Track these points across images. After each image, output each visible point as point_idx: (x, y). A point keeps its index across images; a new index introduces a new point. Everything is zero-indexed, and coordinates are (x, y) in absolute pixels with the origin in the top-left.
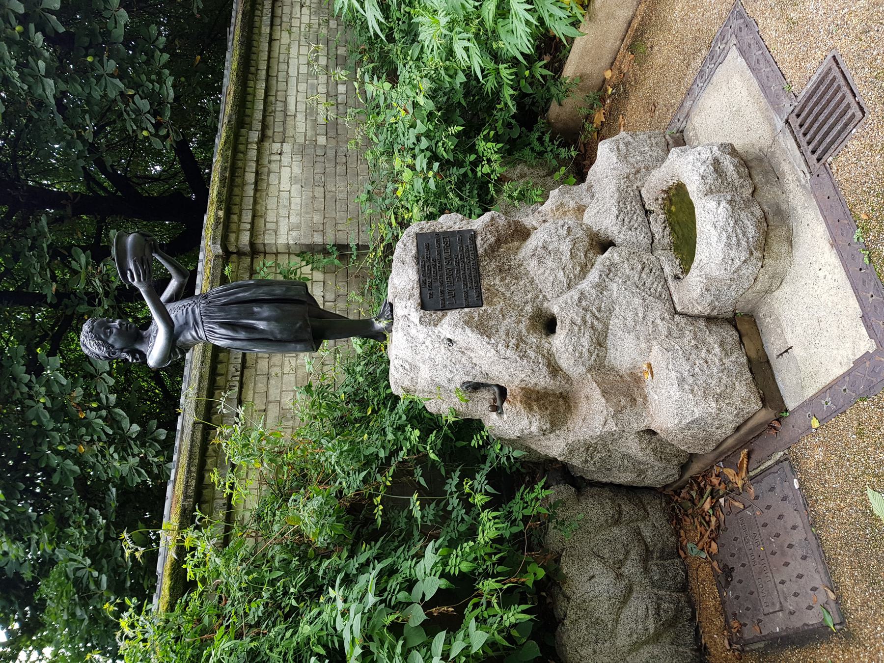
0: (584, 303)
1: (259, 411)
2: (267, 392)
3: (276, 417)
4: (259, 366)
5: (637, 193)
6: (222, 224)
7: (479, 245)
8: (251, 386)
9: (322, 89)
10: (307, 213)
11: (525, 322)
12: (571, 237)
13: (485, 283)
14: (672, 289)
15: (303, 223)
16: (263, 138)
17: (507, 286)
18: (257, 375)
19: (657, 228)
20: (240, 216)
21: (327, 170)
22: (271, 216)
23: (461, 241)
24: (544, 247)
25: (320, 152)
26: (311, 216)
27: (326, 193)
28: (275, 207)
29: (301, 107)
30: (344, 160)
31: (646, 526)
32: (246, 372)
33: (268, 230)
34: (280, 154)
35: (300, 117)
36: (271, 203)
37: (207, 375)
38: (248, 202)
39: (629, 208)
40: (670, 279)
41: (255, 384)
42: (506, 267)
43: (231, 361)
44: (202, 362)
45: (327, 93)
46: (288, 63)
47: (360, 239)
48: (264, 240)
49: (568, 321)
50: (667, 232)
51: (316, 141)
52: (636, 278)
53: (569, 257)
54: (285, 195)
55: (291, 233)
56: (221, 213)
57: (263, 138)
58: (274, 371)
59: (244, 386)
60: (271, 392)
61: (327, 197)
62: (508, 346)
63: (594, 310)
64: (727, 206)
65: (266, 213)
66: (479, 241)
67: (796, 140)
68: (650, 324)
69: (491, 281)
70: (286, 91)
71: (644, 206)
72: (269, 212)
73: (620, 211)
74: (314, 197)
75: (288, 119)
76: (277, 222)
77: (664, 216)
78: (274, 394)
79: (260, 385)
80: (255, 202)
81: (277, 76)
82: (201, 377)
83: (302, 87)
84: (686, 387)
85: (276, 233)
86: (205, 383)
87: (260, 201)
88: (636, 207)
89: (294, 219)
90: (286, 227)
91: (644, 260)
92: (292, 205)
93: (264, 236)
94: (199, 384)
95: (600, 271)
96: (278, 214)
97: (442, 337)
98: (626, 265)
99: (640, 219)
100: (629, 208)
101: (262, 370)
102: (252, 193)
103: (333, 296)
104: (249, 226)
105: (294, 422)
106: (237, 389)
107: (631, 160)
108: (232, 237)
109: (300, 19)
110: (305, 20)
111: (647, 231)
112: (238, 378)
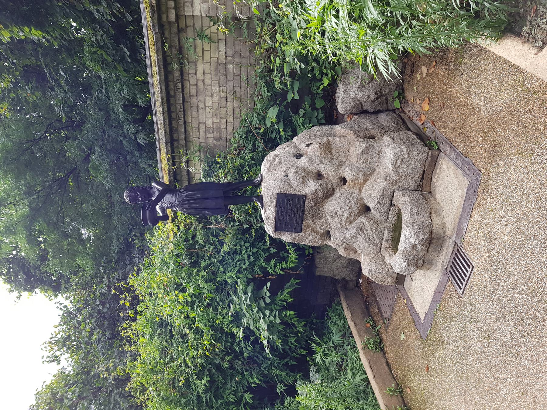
2: (198, 117)
3: (204, 131)
4: (192, 101)
5: (392, 194)
6: (156, 12)
7: (306, 206)
8: (189, 113)
11: (318, 237)
12: (350, 210)
13: (304, 223)
14: (383, 243)
17: (315, 223)
18: (191, 107)
19: (391, 215)
23: (299, 201)
24: (336, 213)
32: (185, 103)
37: (167, 117)
39: (384, 201)
40: (384, 239)
41: (191, 112)
42: (316, 214)
43: (177, 102)
44: (163, 109)
47: (250, 14)
48: (184, 12)
49: (335, 243)
50: (394, 219)
52: (371, 235)
53: (345, 219)
55: (202, 5)
58: (201, 105)
60: (200, 117)
64: (406, 265)
66: (306, 203)
68: (368, 251)
69: (308, 221)
71: (392, 201)
73: (379, 202)
77: (397, 211)
78: (202, 118)
79: (194, 113)
82: (164, 118)
84: (371, 274)
86: (167, 122)
88: (388, 201)
91: (378, 228)
93: (184, 8)
94: (164, 123)
95: (356, 230)
98: (369, 228)
99: (386, 208)
100: (384, 201)
101: (194, 104)
103: (231, 53)
105: (213, 135)
106: (183, 119)
107: (400, 170)
108: (164, 17)
111: (386, 215)
112: (182, 113)
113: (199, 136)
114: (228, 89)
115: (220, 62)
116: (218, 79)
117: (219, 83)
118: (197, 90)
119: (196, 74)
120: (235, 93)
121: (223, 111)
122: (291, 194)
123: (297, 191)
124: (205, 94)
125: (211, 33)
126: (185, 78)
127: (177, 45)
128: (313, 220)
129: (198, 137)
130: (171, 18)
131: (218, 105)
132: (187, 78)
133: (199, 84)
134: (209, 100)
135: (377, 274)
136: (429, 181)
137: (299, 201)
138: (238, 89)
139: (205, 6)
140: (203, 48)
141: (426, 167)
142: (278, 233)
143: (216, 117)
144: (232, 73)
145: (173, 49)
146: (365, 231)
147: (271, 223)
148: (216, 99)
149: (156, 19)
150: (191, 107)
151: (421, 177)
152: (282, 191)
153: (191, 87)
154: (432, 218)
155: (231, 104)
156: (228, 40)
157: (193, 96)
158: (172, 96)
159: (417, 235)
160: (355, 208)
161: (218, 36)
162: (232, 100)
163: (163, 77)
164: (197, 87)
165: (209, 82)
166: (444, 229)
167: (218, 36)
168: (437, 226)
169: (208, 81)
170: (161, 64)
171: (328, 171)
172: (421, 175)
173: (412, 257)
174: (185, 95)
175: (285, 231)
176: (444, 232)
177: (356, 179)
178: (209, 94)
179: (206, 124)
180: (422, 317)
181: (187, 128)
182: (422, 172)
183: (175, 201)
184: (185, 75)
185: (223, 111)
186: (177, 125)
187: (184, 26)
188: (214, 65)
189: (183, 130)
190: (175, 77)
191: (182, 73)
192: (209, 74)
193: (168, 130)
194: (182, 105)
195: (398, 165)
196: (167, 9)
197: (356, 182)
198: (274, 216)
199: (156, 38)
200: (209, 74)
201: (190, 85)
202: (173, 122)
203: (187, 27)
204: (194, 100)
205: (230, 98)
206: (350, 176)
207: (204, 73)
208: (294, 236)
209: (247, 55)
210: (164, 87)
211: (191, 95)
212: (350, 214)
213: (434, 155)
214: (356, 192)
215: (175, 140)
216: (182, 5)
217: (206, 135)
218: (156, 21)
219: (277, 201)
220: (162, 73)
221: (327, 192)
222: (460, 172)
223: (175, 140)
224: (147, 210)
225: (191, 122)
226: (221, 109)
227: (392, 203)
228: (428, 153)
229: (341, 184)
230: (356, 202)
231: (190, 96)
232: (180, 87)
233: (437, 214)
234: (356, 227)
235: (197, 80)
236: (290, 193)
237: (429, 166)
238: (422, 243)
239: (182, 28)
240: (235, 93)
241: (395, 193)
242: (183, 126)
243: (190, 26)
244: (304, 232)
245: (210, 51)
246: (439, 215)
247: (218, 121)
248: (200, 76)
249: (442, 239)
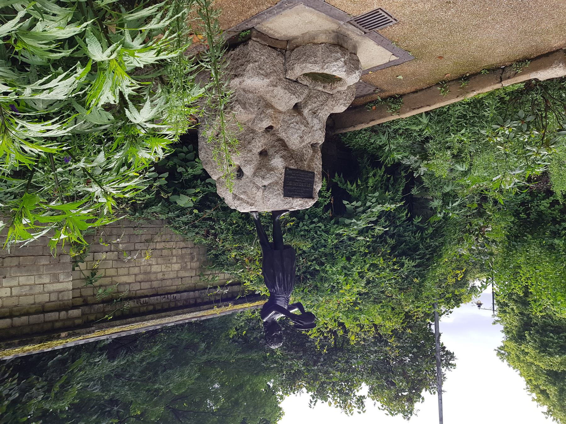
1: (182, 281)
5: (288, 81)
6: (75, 331)
7: (294, 168)
8: (168, 288)
10: (38, 270)
12: (299, 123)
13: (307, 169)
14: (326, 91)
15: (51, 272)
17: (306, 159)
18: (162, 286)
20: (53, 322)
22: (45, 298)
24: (301, 137)
26: (41, 267)
27: (12, 255)
28: (32, 297)
32: (159, 293)
33: (58, 298)
36: (26, 301)
38: (34, 318)
40: (323, 90)
41: (167, 286)
43: (159, 302)
44: (169, 316)
48: (69, 300)
54: (15, 291)
55: (61, 280)
56: (63, 335)
58: (160, 276)
59: (168, 292)
60: (172, 277)
61: (17, 254)
65: (39, 303)
66: (292, 167)
67: (353, 25)
69: (305, 166)
72: (37, 301)
73: (294, 95)
74: (19, 266)
76: (50, 293)
78: (172, 275)
80: (28, 314)
85: (64, 291)
86: (180, 311)
87: (25, 310)
89: (46, 280)
90: (55, 285)
92: (28, 283)
93: (65, 300)
94: (181, 314)
95: (315, 118)
96: (40, 293)
102: (24, 319)
104: (63, 314)
106: (175, 295)
108: (78, 322)
113: (189, 276)
114: (144, 248)
115: (116, 258)
118: (145, 282)
119: (129, 284)
120: (147, 241)
121: (165, 252)
122: (284, 182)
123: (281, 176)
124: (150, 273)
125: (87, 269)
126: (134, 295)
127: (101, 305)
128: (304, 160)
129: (190, 278)
130: (77, 314)
131: (160, 259)
132: (134, 292)
133: (140, 280)
134: (155, 268)
135: (348, 98)
136: (277, 41)
137: (290, 175)
138: (144, 238)
139: (62, 277)
140: (103, 277)
141: (266, 44)
142: (314, 195)
143: (171, 260)
144: (128, 244)
145: (107, 309)
146: (316, 109)
147: (306, 202)
149: (82, 330)
150: (162, 286)
151: (273, 50)
152: (281, 191)
153: (142, 288)
154: (319, 43)
156: (93, 249)
157: (151, 285)
158: (154, 308)
159: (337, 60)
160: (298, 118)
161: (89, 261)
162: (154, 243)
163: (138, 318)
165: (137, 269)
166: (330, 32)
167: (89, 261)
168: (327, 38)
169: (136, 270)
170: (124, 321)
171: (259, 144)
172: (272, 49)
173: (352, 65)
174: (151, 294)
175: (312, 188)
176: (334, 32)
177: (271, 117)
179: (178, 270)
180: (394, 58)
181: (182, 290)
182: (270, 48)
183: (284, 297)
184: (131, 295)
186: (181, 300)
187: (81, 299)
188: (119, 265)
189: (185, 294)
190: (135, 306)
191: (129, 298)
192: (129, 269)
193: (187, 309)
194: (162, 297)
195: (264, 73)
196: (69, 319)
197: (273, 116)
198: (301, 199)
199: (99, 329)
200: (129, 269)
201: (141, 289)
202: (179, 304)
203: (81, 296)
204: (155, 284)
205: (152, 245)
206: (268, 122)
207: (129, 274)
208: (317, 180)
209: (108, 229)
210: (147, 317)
211: (150, 287)
212: (302, 123)
213: (256, 35)
214: (282, 117)
215: (196, 302)
216: (61, 303)
217: (188, 270)
218: (84, 330)
219: (290, 197)
220: (133, 319)
221: (282, 146)
222: (288, 11)
223: (196, 302)
224: (303, 324)
225: (177, 286)
226: (163, 254)
227: (295, 81)
228: (254, 41)
229: (271, 132)
230: (292, 117)
231: (151, 288)
232: (144, 299)
233: (316, 37)
234: (312, 118)
235: (136, 282)
236: (283, 184)
237: (265, 41)
238: (344, 55)
239: (83, 301)
240: (147, 241)
241: (287, 77)
242: (182, 294)
243: (80, 292)
244: (314, 169)
245: (105, 269)
246: (317, 35)
247: (175, 258)
248: (130, 279)
249: (338, 34)
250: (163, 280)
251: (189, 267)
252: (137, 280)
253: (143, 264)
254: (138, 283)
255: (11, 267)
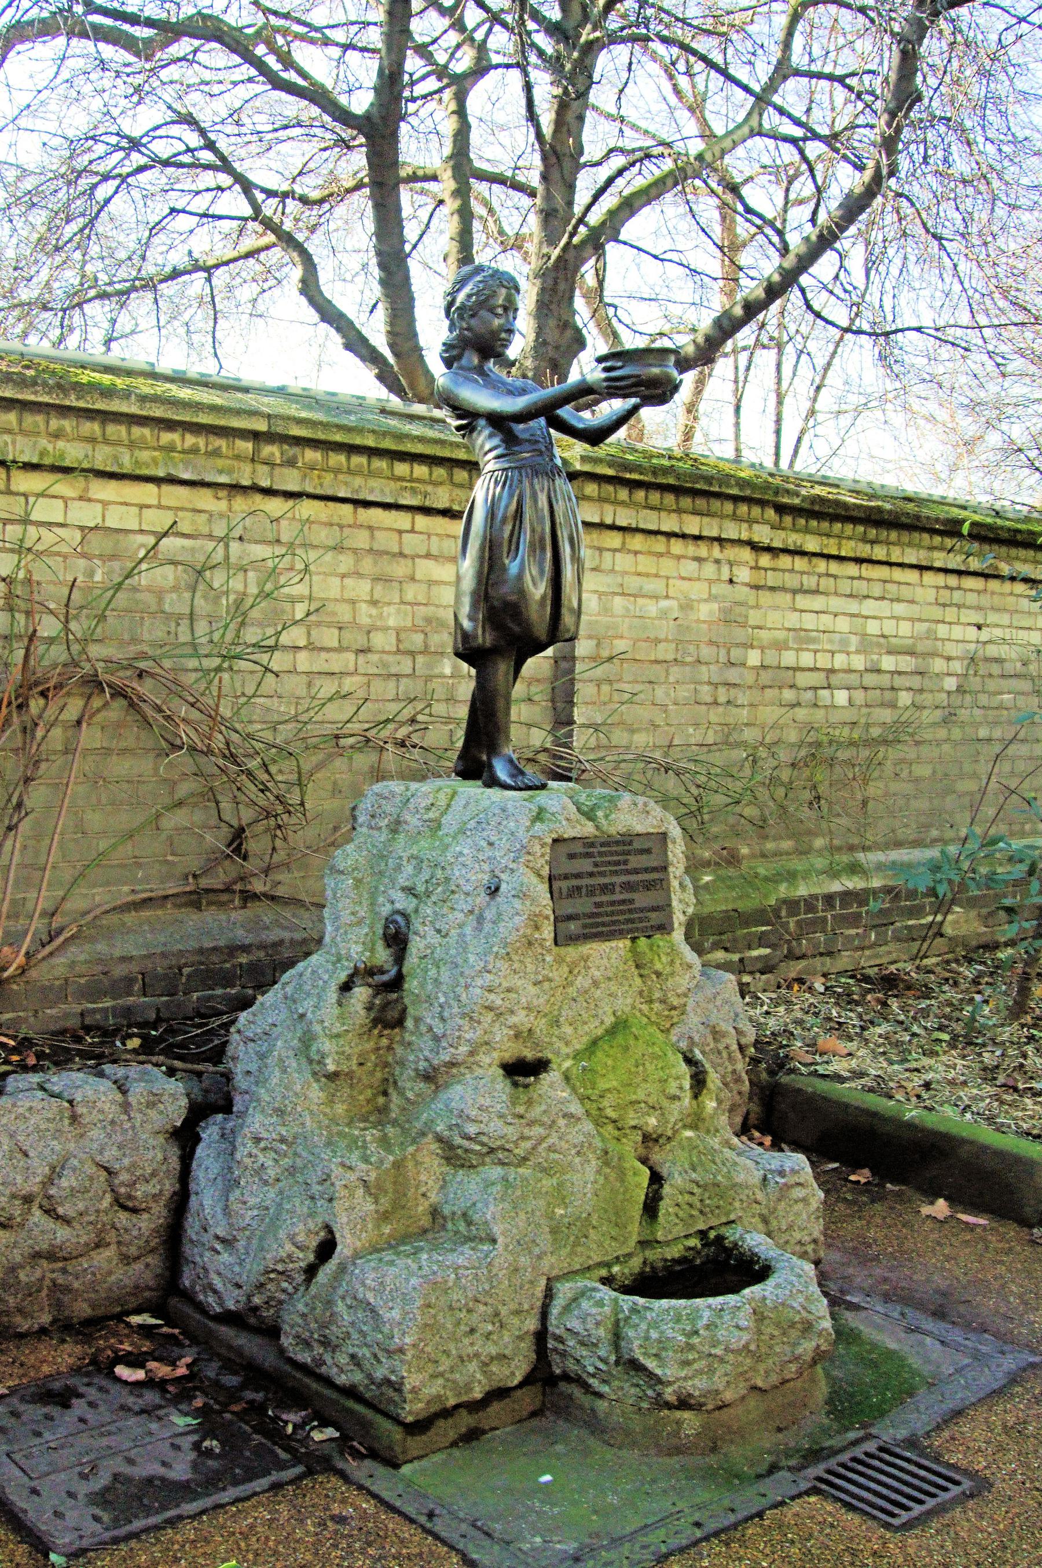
0: (562, 1122)
9: (840, 661)
16: (755, 547)
21: (704, 668)
25: (736, 654)
28: (641, 569)
29: (809, 621)
30: (722, 699)
31: (109, 1260)
34: (731, 581)
35: (793, 620)
45: (832, 671)
46: (883, 598)
51: (752, 647)
57: (755, 547)
62: (490, 991)
63: (550, 1141)
70: (836, 593)
75: (789, 597)
81: (860, 578)
83: (843, 624)
97: (503, 876)
104: (608, 521)
109: (958, 623)
110: (957, 632)
113: (249, 542)
116: (415, 629)
117: (405, 629)
118: (387, 553)
119: (428, 556)
124: (376, 579)
133: (402, 561)
134: (362, 588)
148: (365, 614)
155: (351, 667)
164: (394, 555)
165: (409, 597)
178: (379, 591)
185: (329, 637)
207: (431, 583)
226: (336, 632)
235: (413, 558)
250: (338, 548)
251: (251, 574)
252: (409, 562)
253: (392, 609)
254: (406, 552)
255: (666, 640)
